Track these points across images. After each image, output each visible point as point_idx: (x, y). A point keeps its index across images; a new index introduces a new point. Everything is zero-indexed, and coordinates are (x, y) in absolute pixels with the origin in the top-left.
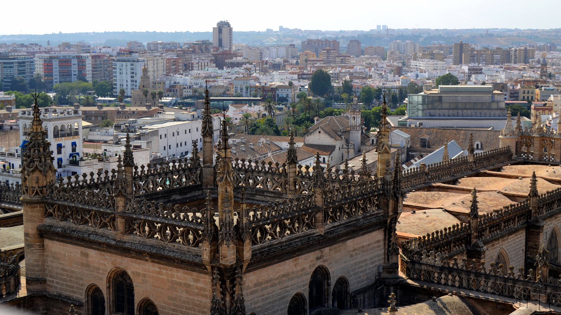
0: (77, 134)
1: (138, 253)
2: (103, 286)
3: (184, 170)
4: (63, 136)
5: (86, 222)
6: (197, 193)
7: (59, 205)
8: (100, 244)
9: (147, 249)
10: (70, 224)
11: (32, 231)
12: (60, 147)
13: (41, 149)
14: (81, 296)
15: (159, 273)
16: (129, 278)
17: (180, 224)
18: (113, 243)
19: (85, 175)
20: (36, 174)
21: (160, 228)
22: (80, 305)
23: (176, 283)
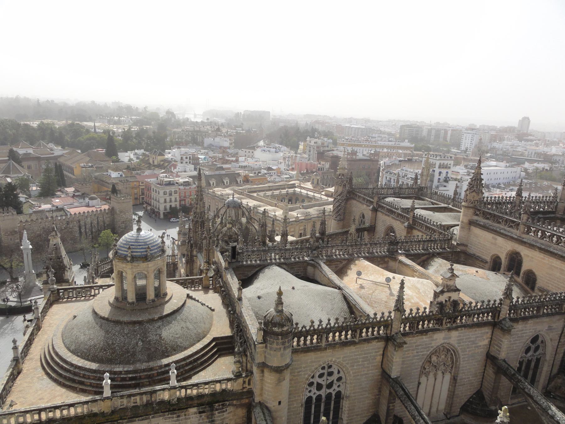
0: (450, 168)
1: (531, 246)
2: (503, 257)
3: (548, 202)
4: (443, 168)
5: (499, 223)
6: (552, 215)
7: (484, 212)
8: (506, 235)
9: (538, 245)
10: (489, 222)
11: (466, 221)
12: (440, 173)
13: (479, 182)
14: (488, 259)
15: (543, 259)
16: (521, 256)
17: (548, 231)
18: (516, 237)
19: (495, 197)
20: (474, 194)
21: (550, 236)
22: (487, 262)
23: (554, 267)
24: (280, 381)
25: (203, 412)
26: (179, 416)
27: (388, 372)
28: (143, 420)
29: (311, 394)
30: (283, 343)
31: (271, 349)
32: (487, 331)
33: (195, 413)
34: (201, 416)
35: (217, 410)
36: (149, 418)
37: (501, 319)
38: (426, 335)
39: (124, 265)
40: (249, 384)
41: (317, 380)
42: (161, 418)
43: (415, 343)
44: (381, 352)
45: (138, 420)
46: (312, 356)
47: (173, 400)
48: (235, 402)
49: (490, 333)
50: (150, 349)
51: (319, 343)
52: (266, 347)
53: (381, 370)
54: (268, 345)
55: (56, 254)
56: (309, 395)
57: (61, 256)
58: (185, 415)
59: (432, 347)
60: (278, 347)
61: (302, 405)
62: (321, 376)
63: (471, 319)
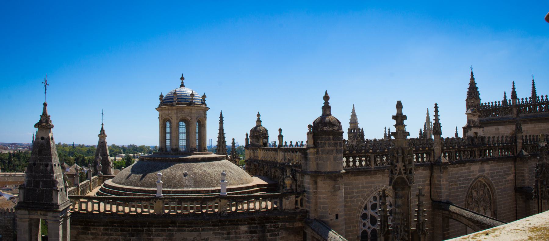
8: (505, 122)
20: (473, 99)
24: (335, 189)
25: (255, 232)
26: (229, 234)
27: (438, 199)
28: (192, 231)
29: (366, 229)
30: (335, 145)
31: (323, 152)
32: (510, 165)
33: (246, 232)
34: (252, 237)
35: (269, 231)
36: (198, 231)
37: (518, 152)
38: (464, 166)
39: (170, 112)
40: (302, 205)
41: (370, 212)
42: (211, 232)
43: (457, 174)
44: (428, 182)
45: (188, 231)
46: (362, 180)
47: (224, 212)
48: (287, 225)
49: (513, 169)
50: (196, 178)
51: (368, 166)
52: (317, 152)
53: (431, 202)
54: (320, 149)
55: (103, 150)
56: (364, 229)
57: (107, 153)
58: (236, 233)
59: (471, 179)
60: (331, 148)
61: (358, 237)
62: (374, 207)
63: (497, 152)
